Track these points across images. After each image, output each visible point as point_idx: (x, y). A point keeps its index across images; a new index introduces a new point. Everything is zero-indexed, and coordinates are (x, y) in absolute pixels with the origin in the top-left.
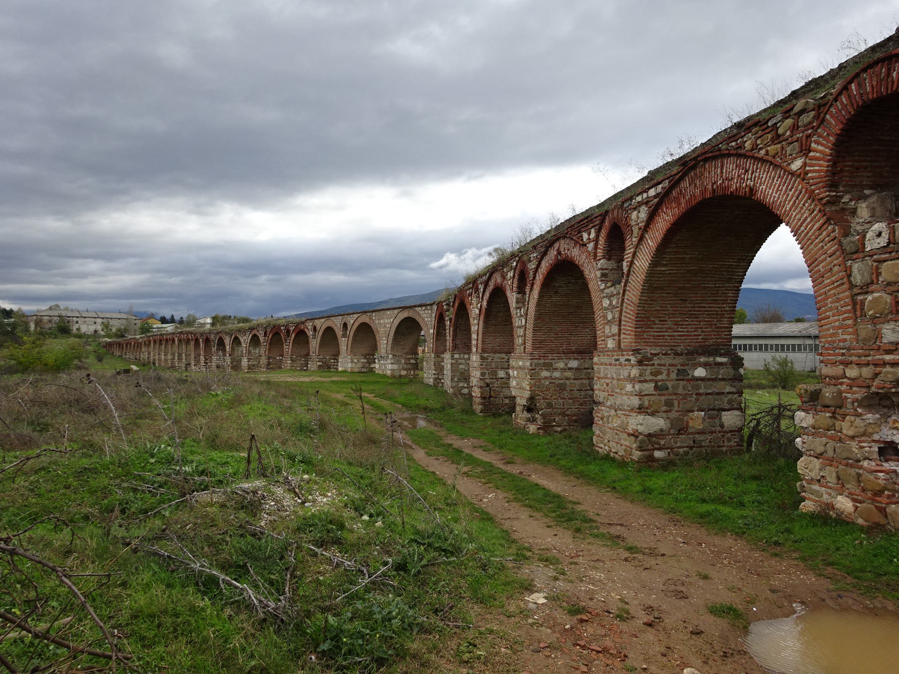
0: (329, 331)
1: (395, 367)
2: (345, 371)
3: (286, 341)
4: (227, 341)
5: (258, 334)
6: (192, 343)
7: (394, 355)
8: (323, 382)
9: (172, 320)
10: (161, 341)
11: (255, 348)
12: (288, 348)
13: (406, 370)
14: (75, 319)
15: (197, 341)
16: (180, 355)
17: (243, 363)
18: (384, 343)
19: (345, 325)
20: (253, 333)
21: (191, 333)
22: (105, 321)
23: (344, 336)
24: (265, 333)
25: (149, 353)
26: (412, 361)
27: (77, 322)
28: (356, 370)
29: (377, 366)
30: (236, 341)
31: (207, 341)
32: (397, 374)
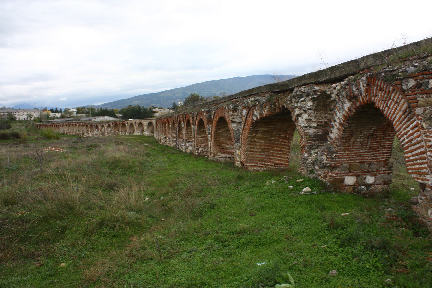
0: (132, 124)
1: (148, 134)
2: (136, 135)
4: (99, 126)
6: (85, 126)
9: (56, 111)
10: (69, 125)
12: (120, 129)
14: (15, 113)
15: (87, 126)
16: (79, 130)
18: (145, 128)
19: (136, 123)
21: (84, 123)
22: (28, 113)
23: (135, 126)
24: (113, 124)
25: (63, 130)
27: (16, 115)
29: (144, 133)
30: (103, 126)
31: (91, 126)
32: (149, 135)
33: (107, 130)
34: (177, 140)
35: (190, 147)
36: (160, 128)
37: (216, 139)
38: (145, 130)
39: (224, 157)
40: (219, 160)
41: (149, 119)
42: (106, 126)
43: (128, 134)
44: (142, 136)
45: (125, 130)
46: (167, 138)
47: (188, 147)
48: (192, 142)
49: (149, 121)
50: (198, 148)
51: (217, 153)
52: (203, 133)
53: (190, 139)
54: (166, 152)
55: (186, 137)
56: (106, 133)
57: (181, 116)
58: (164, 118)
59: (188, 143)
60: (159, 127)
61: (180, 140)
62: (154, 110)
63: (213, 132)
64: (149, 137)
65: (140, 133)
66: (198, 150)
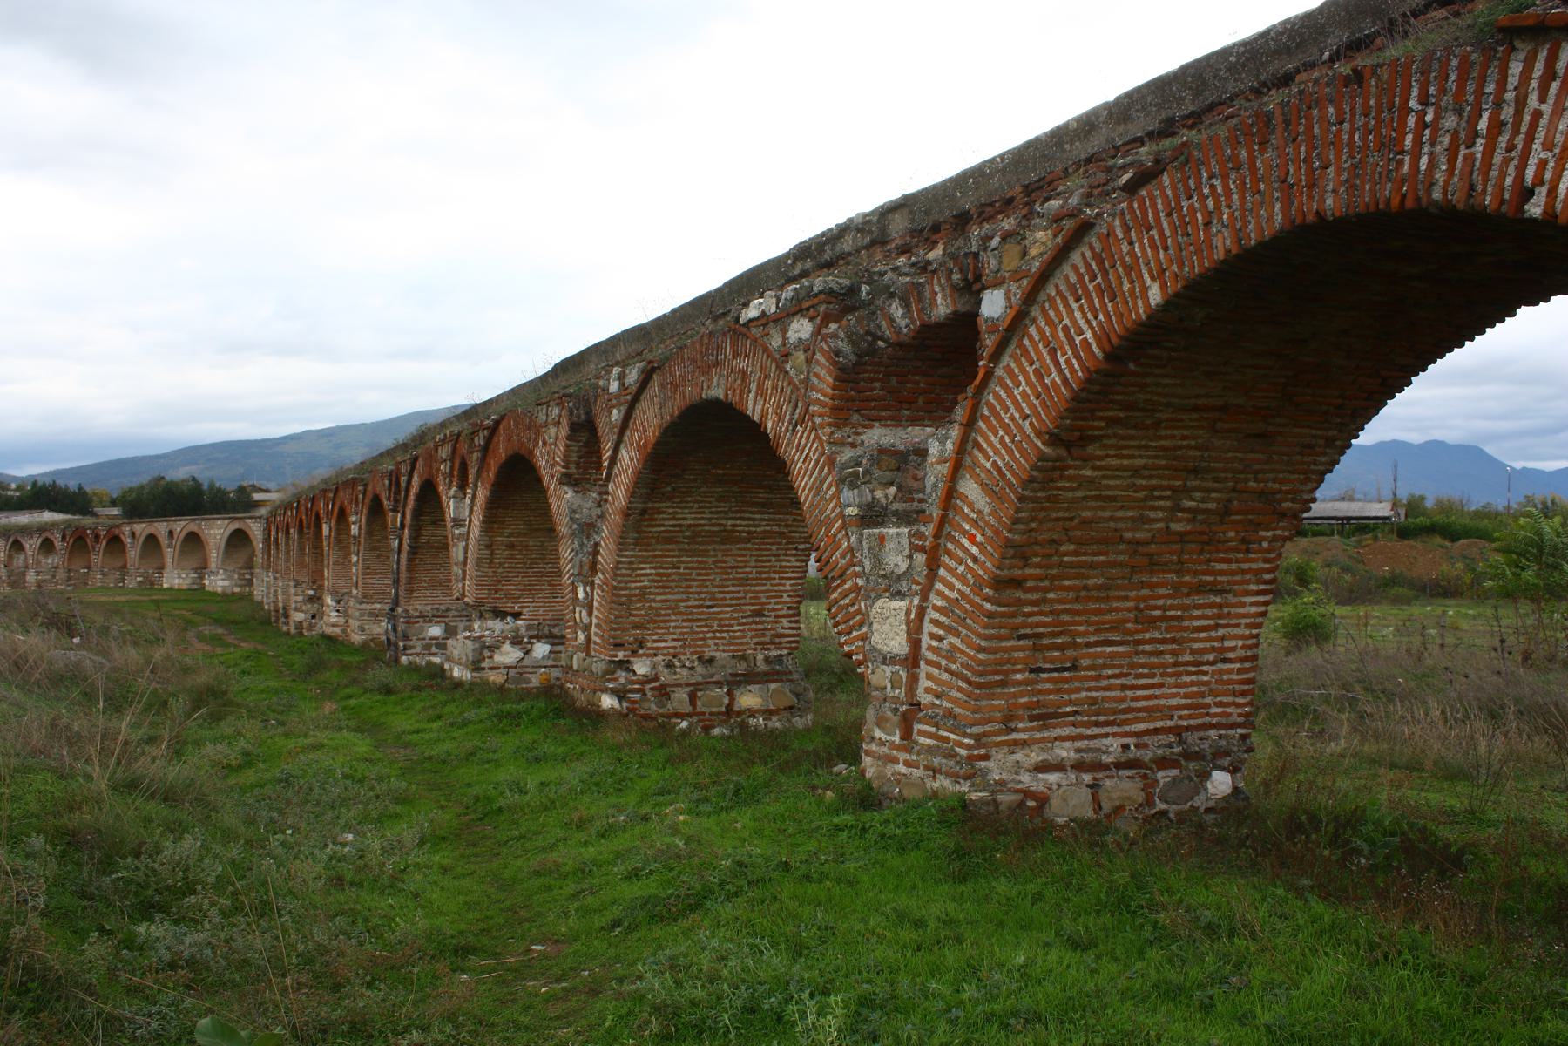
0: (152, 539)
1: (226, 583)
2: (171, 589)
3: (94, 548)
5: (52, 538)
7: (225, 570)
8: (141, 601)
11: (46, 557)
12: (97, 558)
13: (241, 586)
17: (28, 578)
18: (214, 556)
19: (171, 533)
20: (44, 536)
23: (169, 546)
24: (64, 538)
26: (247, 577)
28: (185, 587)
29: (206, 582)
32: (229, 591)
33: (38, 563)
34: (396, 603)
35: (507, 647)
36: (288, 552)
37: (1026, 561)
38: (213, 564)
39: (1079, 766)
40: (1043, 800)
41: (235, 519)
42: (31, 545)
43: (131, 583)
44: (197, 592)
45: (120, 564)
46: (329, 600)
47: (494, 648)
48: (517, 616)
49: (236, 526)
50: (621, 655)
51: (1008, 721)
52: (670, 541)
53: (509, 595)
54: (332, 675)
55: (479, 582)
56: (31, 577)
57: (444, 452)
58: (313, 499)
59: (490, 624)
60: (282, 547)
61: (417, 606)
62: (257, 497)
63: (970, 488)
64: (226, 597)
65: (189, 581)
66: (622, 676)
